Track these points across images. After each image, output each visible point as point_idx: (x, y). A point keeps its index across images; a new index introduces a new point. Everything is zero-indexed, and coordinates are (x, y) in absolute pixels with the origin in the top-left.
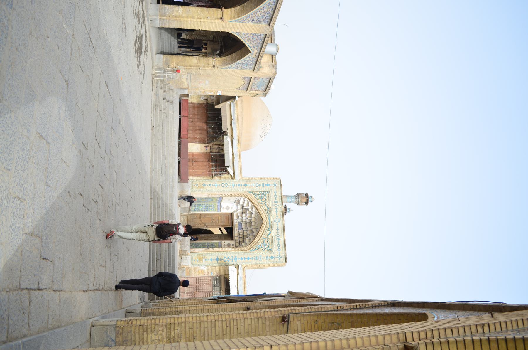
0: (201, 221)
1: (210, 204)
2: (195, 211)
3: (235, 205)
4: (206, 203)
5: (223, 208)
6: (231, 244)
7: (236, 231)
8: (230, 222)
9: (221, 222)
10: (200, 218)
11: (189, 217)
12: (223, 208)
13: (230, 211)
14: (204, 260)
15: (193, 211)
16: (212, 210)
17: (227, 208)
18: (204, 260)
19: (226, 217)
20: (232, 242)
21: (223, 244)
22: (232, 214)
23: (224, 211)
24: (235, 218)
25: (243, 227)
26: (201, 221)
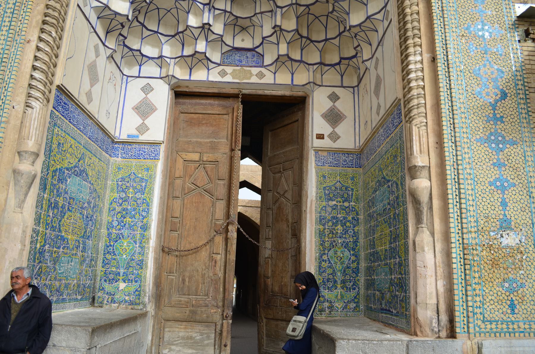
0: (197, 250)
1: (109, 195)
2: (139, 279)
3: (134, 71)
4: (105, 218)
5: (143, 129)
6: (328, 104)
7: (265, 79)
8: (213, 106)
9: (213, 147)
10: (184, 254)
11: (170, 312)
12: (143, 129)
13: (162, 95)
14: (510, 240)
15: (139, 293)
16: (144, 187)
17: (145, 109)
18: (510, 240)
19: (191, 123)
20: (319, 103)
21: (326, 143)
22: (181, 94)
23: (157, 128)
24: (200, 75)
25: (248, 44)
26: (197, 250)
